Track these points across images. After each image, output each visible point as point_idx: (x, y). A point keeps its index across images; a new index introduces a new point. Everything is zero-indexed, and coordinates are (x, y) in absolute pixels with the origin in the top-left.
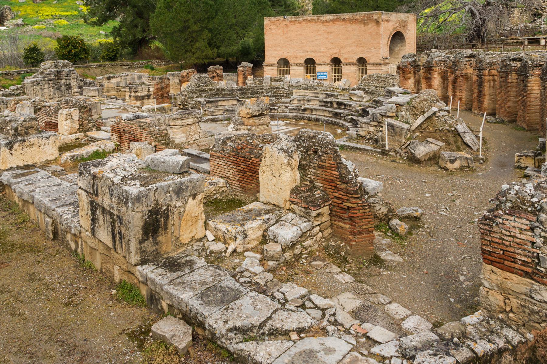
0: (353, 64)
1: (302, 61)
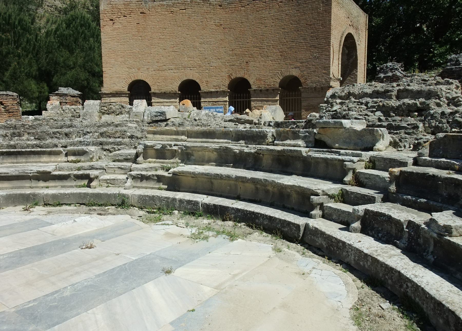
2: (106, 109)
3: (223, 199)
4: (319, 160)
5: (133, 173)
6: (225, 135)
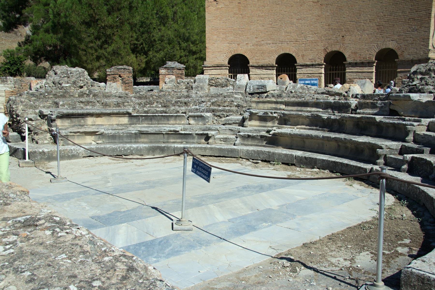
1: (272, 60)
2: (213, 82)
3: (313, 153)
4: (389, 125)
5: (242, 134)
6: (317, 105)
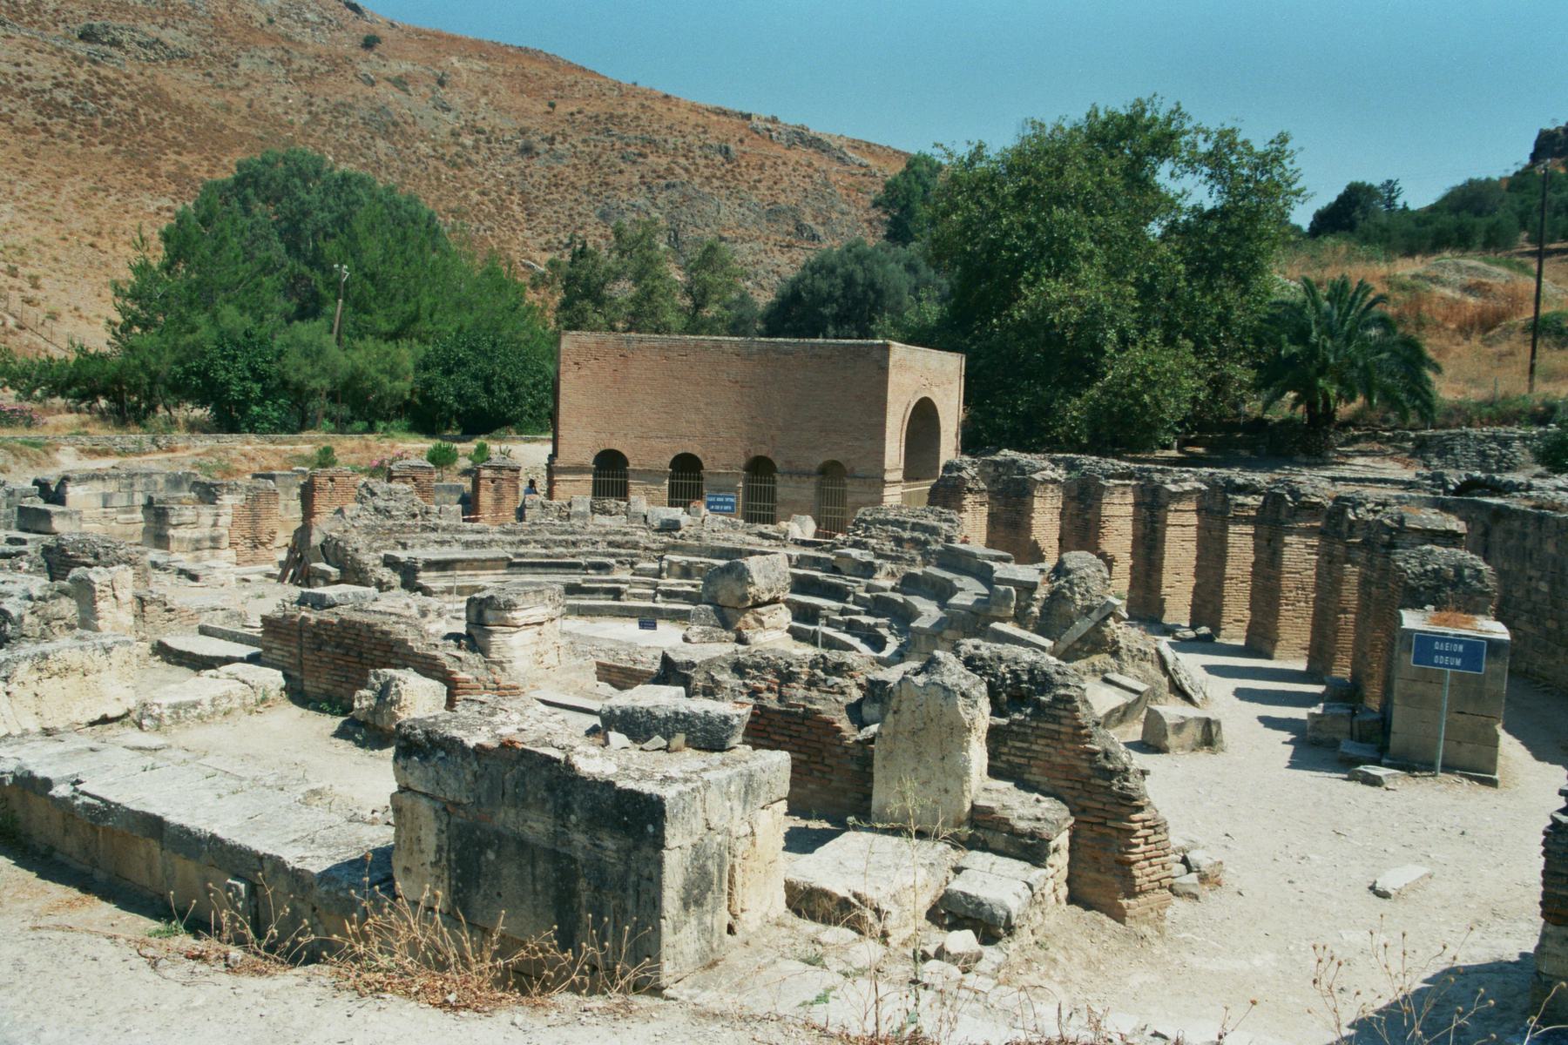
0: (809, 475)
